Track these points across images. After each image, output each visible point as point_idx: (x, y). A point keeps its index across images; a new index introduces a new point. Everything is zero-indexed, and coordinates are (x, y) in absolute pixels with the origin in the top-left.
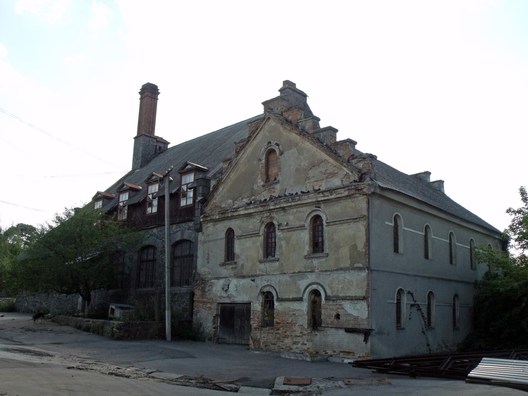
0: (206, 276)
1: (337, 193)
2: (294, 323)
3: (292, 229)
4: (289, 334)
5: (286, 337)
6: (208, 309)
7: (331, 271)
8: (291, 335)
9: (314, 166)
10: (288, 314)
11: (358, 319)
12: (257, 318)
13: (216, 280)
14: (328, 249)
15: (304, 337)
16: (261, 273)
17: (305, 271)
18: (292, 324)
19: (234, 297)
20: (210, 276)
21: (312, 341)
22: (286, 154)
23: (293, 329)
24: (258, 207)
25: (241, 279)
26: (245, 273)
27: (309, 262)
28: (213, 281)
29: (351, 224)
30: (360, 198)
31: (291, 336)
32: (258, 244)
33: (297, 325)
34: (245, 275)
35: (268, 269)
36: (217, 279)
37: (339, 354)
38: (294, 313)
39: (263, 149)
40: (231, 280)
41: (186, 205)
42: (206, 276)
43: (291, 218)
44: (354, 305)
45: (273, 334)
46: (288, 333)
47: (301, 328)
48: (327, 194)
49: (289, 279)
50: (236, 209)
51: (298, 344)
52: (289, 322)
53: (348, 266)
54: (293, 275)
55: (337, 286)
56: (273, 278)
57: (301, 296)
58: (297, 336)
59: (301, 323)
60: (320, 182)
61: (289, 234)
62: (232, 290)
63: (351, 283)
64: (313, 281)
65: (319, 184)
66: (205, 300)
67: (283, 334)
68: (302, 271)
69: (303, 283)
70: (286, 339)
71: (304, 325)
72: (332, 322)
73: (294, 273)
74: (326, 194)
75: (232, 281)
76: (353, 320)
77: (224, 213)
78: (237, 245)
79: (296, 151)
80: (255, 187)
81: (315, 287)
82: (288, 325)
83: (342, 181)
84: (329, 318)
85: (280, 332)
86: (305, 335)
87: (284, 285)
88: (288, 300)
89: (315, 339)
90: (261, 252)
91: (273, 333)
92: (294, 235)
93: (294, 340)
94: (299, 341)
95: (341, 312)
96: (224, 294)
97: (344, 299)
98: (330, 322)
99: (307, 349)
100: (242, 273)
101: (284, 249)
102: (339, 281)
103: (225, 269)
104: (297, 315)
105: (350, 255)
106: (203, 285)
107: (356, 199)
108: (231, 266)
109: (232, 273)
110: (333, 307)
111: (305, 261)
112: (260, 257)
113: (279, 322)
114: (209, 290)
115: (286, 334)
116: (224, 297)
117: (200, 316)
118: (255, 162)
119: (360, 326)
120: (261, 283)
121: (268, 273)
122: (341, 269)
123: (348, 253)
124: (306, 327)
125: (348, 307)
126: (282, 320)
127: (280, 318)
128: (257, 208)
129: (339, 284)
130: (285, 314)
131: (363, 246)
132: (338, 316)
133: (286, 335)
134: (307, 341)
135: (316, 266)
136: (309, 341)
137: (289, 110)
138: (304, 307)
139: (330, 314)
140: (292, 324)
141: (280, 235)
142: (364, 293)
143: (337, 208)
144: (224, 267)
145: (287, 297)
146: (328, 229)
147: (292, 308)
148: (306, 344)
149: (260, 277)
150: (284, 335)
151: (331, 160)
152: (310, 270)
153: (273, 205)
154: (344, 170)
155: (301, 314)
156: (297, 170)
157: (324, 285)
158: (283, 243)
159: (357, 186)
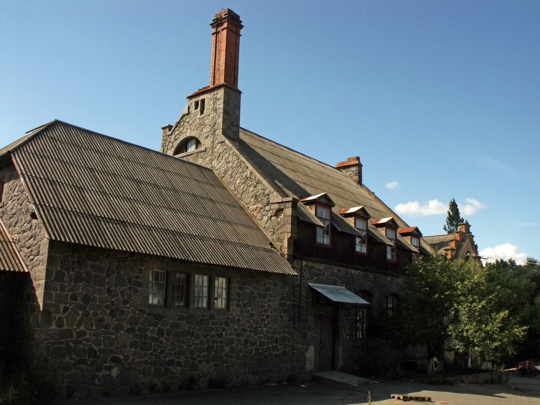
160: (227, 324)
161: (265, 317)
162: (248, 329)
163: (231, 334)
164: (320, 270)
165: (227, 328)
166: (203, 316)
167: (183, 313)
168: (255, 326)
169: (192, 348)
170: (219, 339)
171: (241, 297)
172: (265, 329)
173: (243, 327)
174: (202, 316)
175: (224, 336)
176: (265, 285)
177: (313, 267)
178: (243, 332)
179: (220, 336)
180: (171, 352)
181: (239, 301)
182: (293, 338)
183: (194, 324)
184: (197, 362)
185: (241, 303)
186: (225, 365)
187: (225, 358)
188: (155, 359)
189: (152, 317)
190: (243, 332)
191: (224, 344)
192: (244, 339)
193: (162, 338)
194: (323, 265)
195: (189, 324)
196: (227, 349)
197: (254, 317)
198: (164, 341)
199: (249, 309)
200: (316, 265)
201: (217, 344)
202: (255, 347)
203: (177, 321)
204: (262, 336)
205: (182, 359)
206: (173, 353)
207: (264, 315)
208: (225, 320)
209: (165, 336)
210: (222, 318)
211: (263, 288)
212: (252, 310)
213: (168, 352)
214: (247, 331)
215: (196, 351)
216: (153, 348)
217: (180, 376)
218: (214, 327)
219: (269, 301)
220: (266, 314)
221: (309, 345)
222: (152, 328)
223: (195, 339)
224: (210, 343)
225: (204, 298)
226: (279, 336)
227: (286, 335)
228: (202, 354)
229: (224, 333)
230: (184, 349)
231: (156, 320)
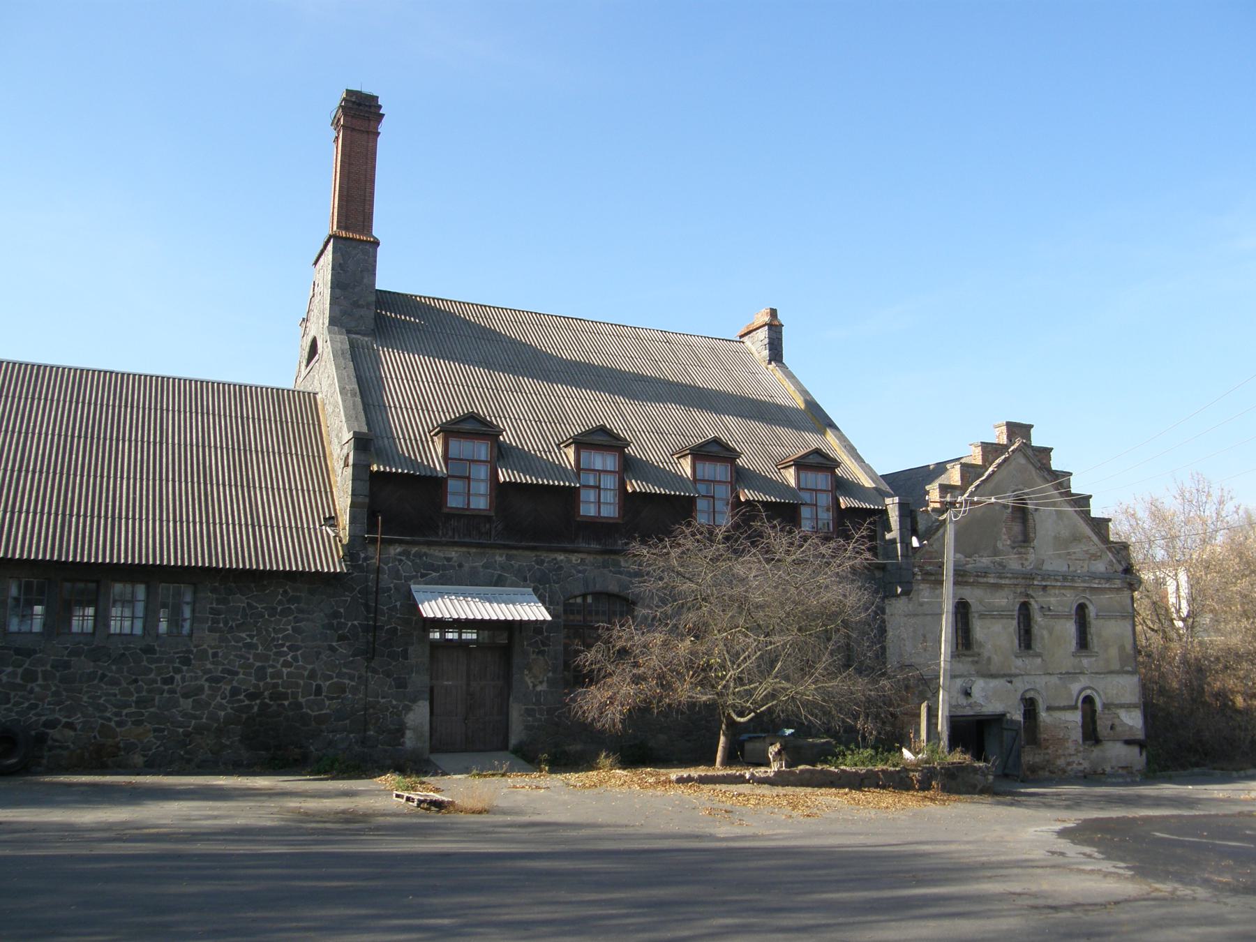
5: (1059, 757)
7: (1104, 673)
16: (1018, 671)
18: (1065, 740)
19: (982, 706)
26: (993, 669)
31: (1064, 755)
46: (1060, 752)
50: (985, 574)
52: (1061, 737)
57: (1073, 703)
59: (1075, 739)
69: (1075, 687)
73: (1061, 674)
74: (1102, 581)
77: (962, 576)
78: (978, 629)
80: (999, 545)
81: (1088, 692)
95: (1116, 722)
96: (963, 701)
97: (1122, 706)
98: (1106, 735)
103: (959, 662)
106: (921, 688)
108: (970, 659)
109: (972, 669)
113: (1047, 738)
116: (965, 707)
120: (1020, 685)
122: (1112, 672)
124: (1080, 741)
132: (1112, 728)
134: (1084, 759)
138: (1076, 717)
140: (1065, 740)
143: (1105, 598)
145: (1057, 705)
148: (1081, 764)
149: (1020, 677)
151: (1095, 538)
152: (1078, 671)
156: (1056, 538)
158: (1045, 633)
160: (186, 661)
161: (285, 649)
162: (241, 671)
163: (196, 678)
164: (449, 559)
165: (185, 668)
166: (126, 649)
167: (81, 645)
168: (258, 664)
169: (101, 701)
170: (166, 687)
171: (223, 616)
172: (285, 670)
173: (228, 667)
174: (124, 649)
175: (178, 682)
176: (285, 592)
177: (426, 554)
178: (226, 675)
179: (170, 680)
180: (52, 707)
181: (215, 621)
182: (366, 686)
183: (105, 662)
184: (113, 724)
185: (221, 625)
186: (181, 730)
187: (180, 719)
188: (16, 717)
189: (12, 652)
190: (226, 675)
191: (179, 694)
192: (229, 688)
193: (34, 685)
194: (456, 549)
195: (94, 661)
196: (186, 704)
197: (257, 650)
198: (37, 689)
199: (244, 635)
200: (435, 550)
201: (162, 694)
202: (258, 702)
203: (65, 658)
204: (277, 683)
205: (78, 719)
206: (57, 708)
207: (283, 645)
208: (181, 655)
209: (40, 682)
210: (172, 651)
211: (280, 597)
212: (251, 637)
213: (46, 706)
214: (237, 673)
215: (109, 706)
216: (12, 701)
217: (72, 746)
218: (153, 666)
219: (297, 620)
220: (287, 644)
221: (414, 701)
222: (10, 669)
223: (108, 687)
224: (144, 694)
225: (135, 621)
226: (328, 683)
227: (347, 681)
228: (125, 712)
229: (178, 677)
230: (83, 703)
231: (20, 657)
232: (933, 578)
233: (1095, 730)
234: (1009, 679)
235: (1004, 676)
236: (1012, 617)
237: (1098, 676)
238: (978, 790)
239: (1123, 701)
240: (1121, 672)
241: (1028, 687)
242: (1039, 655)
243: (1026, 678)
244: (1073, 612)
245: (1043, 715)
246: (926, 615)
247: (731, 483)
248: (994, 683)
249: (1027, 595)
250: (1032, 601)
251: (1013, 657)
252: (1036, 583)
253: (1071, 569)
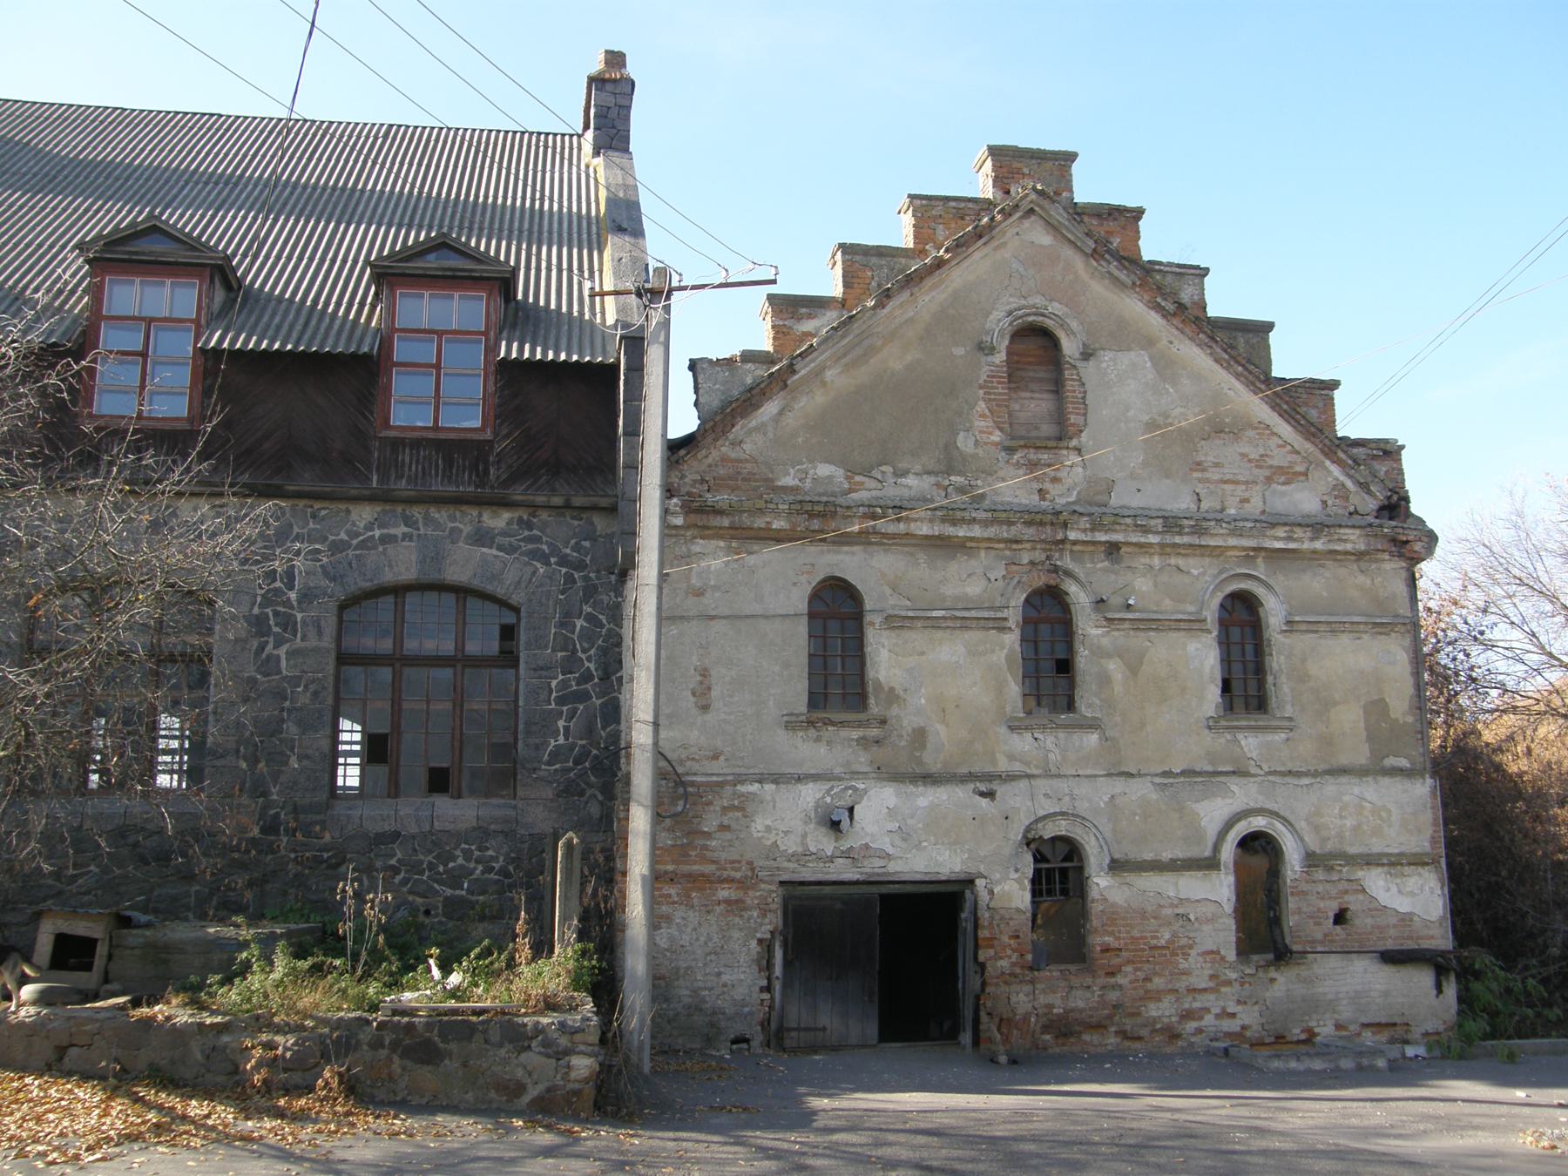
0: (696, 767)
1: (1336, 537)
2: (1182, 948)
3: (1152, 624)
4: (1162, 987)
5: (1156, 996)
6: (718, 909)
7: (1315, 774)
8: (1170, 987)
9: (1222, 431)
10: (1155, 918)
11: (1411, 920)
12: (1011, 937)
13: (770, 787)
14: (1293, 705)
15: (1223, 989)
16: (1017, 767)
17: (1209, 768)
18: (1175, 950)
20: (719, 767)
21: (1256, 1003)
22: (1107, 356)
23: (1181, 966)
24: (1013, 523)
25: (921, 789)
26: (932, 760)
27: (1222, 740)
28: (755, 788)
29: (1365, 637)
30: (1388, 566)
32: (1000, 657)
33: (1193, 952)
34: (934, 770)
35: (1052, 756)
36: (776, 782)
37: (1359, 1034)
38: (1180, 911)
39: (998, 314)
40: (865, 791)
41: (436, 428)
42: (689, 763)
43: (1143, 584)
44: (1398, 881)
45: (1094, 992)
46: (1158, 982)
47: (1213, 962)
48: (1301, 535)
49: (1154, 796)
51: (1201, 1018)
52: (1163, 942)
53: (1364, 761)
54: (1166, 781)
55: (1338, 822)
56: (1083, 789)
57: (1207, 853)
58: (1195, 990)
59: (1210, 946)
60: (1244, 487)
61: (1139, 640)
62: (872, 829)
63: (1384, 814)
64: (1252, 805)
65: (1238, 492)
66: (709, 869)
67: (1135, 989)
68: (1198, 769)
69: (1212, 812)
70: (1152, 1006)
71: (1223, 952)
72: (1326, 935)
74: (1299, 532)
75: (872, 793)
76: (1395, 926)
78: (884, 654)
79: (1149, 364)
80: (964, 443)
81: (1259, 823)
82: (1156, 953)
83: (1324, 502)
84: (1319, 924)
85: (1120, 980)
86: (1228, 983)
87: (1135, 814)
88: (1157, 866)
89: (1268, 994)
90: (1014, 689)
91: (1088, 987)
92: (1160, 649)
93: (1187, 1006)
94: (1207, 1005)
95: (1354, 903)
96: (825, 843)
97: (1370, 861)
98: (1319, 936)
99: (1238, 1029)
100: (920, 762)
101: (1118, 689)
102: (1341, 809)
103: (818, 739)
104: (1192, 917)
105: (1367, 729)
107: (1374, 566)
108: (856, 734)
109: (862, 761)
110: (1328, 886)
111: (1208, 736)
112: (1008, 709)
113: (1116, 945)
114: (724, 828)
115: (1149, 986)
117: (671, 939)
118: (959, 351)
119: (1421, 941)
121: (1054, 771)
122: (1343, 771)
123: (1362, 725)
124: (1231, 954)
125: (1381, 888)
126: (1132, 938)
127: (1119, 932)
128: (1005, 527)
129: (1345, 818)
130: (1143, 915)
131: (1406, 708)
133: (1147, 992)
134: (1239, 1002)
135: (1254, 755)
136: (1245, 1003)
137: (1110, 214)
138: (1220, 889)
139: (1319, 909)
140: (1175, 950)
141: (1098, 636)
142: (1427, 844)
143: (1315, 584)
144: (812, 733)
145: (1148, 856)
146: (1287, 641)
147: (1171, 894)
148: (1233, 1015)
149: (1023, 784)
150: (1141, 992)
151: (1285, 429)
153: (1085, 531)
154: (1329, 472)
155: (1209, 915)
157: (1291, 818)
158: (1114, 667)
159: (1401, 531)
232: (726, 522)
233: (1275, 922)
234: (983, 787)
235: (971, 777)
236: (1000, 626)
237: (1289, 779)
238: (526, 1099)
239: (1377, 846)
240: (1376, 770)
241: (1049, 807)
242: (1092, 725)
243: (1042, 785)
244: (1211, 613)
245: (1101, 883)
246: (712, 618)
247: (197, 321)
248: (926, 798)
249: (1055, 570)
250: (1072, 588)
251: (1003, 730)
252: (1072, 535)
253: (1205, 505)
